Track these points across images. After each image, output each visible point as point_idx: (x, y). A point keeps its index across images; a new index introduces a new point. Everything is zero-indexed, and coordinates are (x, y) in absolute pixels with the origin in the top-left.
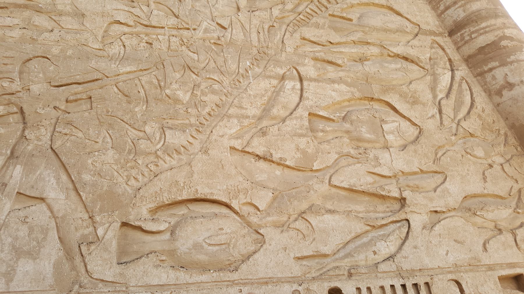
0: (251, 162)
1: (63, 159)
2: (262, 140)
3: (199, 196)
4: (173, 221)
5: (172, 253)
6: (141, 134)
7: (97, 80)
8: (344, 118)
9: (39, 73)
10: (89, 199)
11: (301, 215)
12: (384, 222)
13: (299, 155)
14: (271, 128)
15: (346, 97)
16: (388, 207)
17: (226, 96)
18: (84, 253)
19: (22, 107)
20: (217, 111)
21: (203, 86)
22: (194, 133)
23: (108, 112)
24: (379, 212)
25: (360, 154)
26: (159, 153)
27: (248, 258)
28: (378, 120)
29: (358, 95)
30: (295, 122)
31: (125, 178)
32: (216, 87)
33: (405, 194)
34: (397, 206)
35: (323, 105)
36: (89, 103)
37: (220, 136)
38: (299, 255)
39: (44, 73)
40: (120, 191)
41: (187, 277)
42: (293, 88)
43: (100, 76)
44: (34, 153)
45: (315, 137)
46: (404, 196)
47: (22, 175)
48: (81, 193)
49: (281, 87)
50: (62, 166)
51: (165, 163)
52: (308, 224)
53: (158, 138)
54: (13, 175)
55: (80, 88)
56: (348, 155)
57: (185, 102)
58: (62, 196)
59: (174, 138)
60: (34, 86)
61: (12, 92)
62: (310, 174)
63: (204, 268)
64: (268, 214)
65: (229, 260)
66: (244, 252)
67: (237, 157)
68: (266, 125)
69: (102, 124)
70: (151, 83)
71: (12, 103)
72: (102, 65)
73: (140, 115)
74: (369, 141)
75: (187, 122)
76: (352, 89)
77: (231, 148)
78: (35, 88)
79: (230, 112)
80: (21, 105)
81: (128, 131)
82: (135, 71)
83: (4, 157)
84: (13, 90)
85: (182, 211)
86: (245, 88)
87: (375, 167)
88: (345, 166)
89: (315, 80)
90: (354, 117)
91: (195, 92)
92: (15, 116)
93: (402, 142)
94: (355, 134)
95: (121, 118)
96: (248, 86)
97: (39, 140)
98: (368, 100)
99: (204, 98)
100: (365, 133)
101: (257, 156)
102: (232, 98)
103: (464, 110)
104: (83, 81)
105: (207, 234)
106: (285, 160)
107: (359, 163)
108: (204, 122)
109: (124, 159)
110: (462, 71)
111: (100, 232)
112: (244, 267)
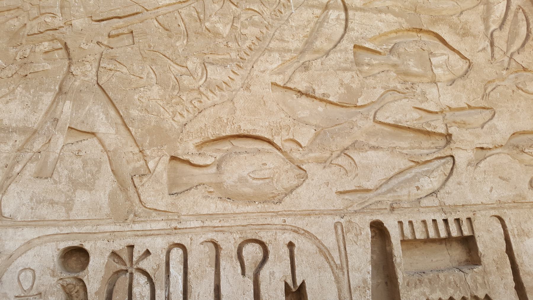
0: (293, 98)
1: (110, 94)
2: (305, 75)
3: (242, 132)
4: (218, 156)
5: (219, 185)
6: (184, 70)
7: (137, 13)
8: (391, 51)
9: (80, 7)
10: (138, 134)
11: (344, 152)
12: (428, 158)
13: (343, 90)
14: (313, 62)
15: (394, 28)
16: (433, 144)
17: (267, 28)
18: (137, 185)
19: (66, 43)
20: (257, 44)
21: (243, 17)
22: (235, 69)
23: (150, 46)
24: (424, 149)
25: (407, 89)
26: (202, 89)
27: (291, 192)
28: (426, 53)
29: (405, 25)
30: (339, 55)
31: (171, 114)
32: (256, 18)
33: (452, 130)
34: (442, 142)
35: (370, 37)
36: (131, 37)
37: (261, 72)
38: (341, 190)
39: (85, 8)
40: (167, 126)
41: (234, 207)
42: (338, 18)
43: (140, 9)
44: (81, 88)
45: (361, 72)
46: (450, 132)
47: (72, 110)
48: (131, 128)
49: (324, 17)
50: (110, 102)
51: (208, 99)
52: (351, 161)
53: (200, 74)
54: (64, 111)
55: (121, 22)
56: (394, 90)
57: (225, 35)
58: (112, 131)
59: (217, 74)
60: (75, 21)
61: (55, 28)
62: (354, 110)
64: (311, 151)
65: (273, 193)
66: (287, 186)
67: (278, 93)
68: (308, 59)
69: (145, 59)
70: (190, 15)
71: (56, 39)
73: (182, 49)
74: (416, 75)
75: (228, 56)
76: (400, 20)
77: (272, 83)
78: (77, 23)
79: (271, 45)
80: (65, 41)
81: (171, 67)
82: (174, 4)
83: (53, 93)
84: (56, 26)
85: (226, 146)
86: (286, 19)
87: (422, 102)
88: (391, 102)
89: (361, 9)
90: (401, 50)
91: (234, 24)
92: (60, 51)
93: (450, 77)
94: (402, 68)
95: (164, 53)
96: (289, 16)
97: (86, 76)
98: (417, 32)
99: (244, 31)
100: (413, 66)
101: (299, 92)
102: (274, 29)
104: (122, 15)
105: (251, 169)
106: (329, 96)
107: (405, 98)
108: (245, 56)
109: (169, 95)
111: (151, 165)
112: (287, 199)
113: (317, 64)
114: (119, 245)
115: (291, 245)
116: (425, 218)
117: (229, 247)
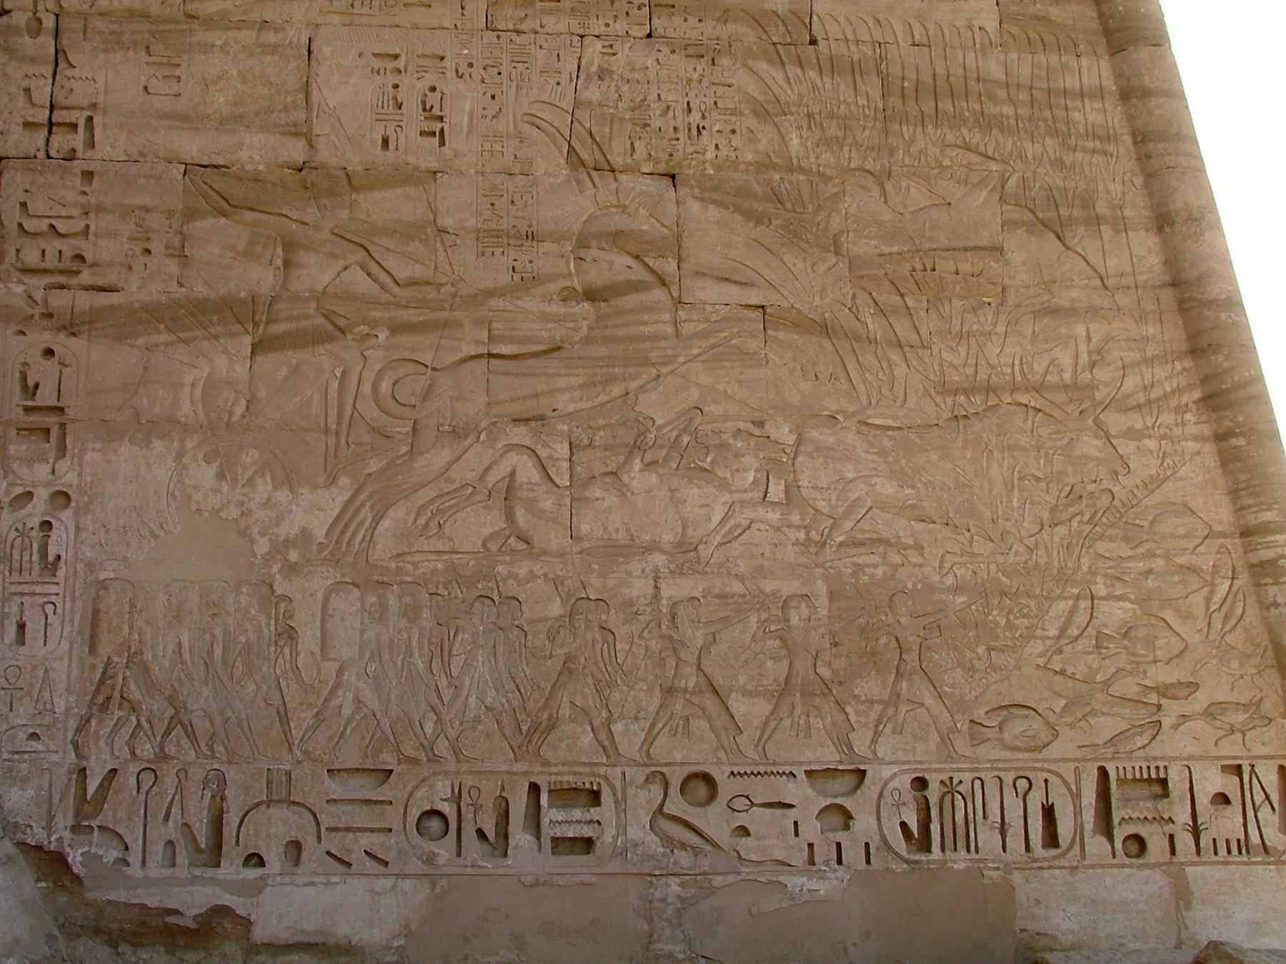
4: (1000, 719)
34: (1154, 709)
63: (1018, 749)
72: (944, 597)
85: (1005, 713)
103: (1232, 622)
110: (1244, 578)
113: (1068, 649)
114: (945, 777)
115: (1046, 781)
116: (1134, 765)
117: (1008, 778)
